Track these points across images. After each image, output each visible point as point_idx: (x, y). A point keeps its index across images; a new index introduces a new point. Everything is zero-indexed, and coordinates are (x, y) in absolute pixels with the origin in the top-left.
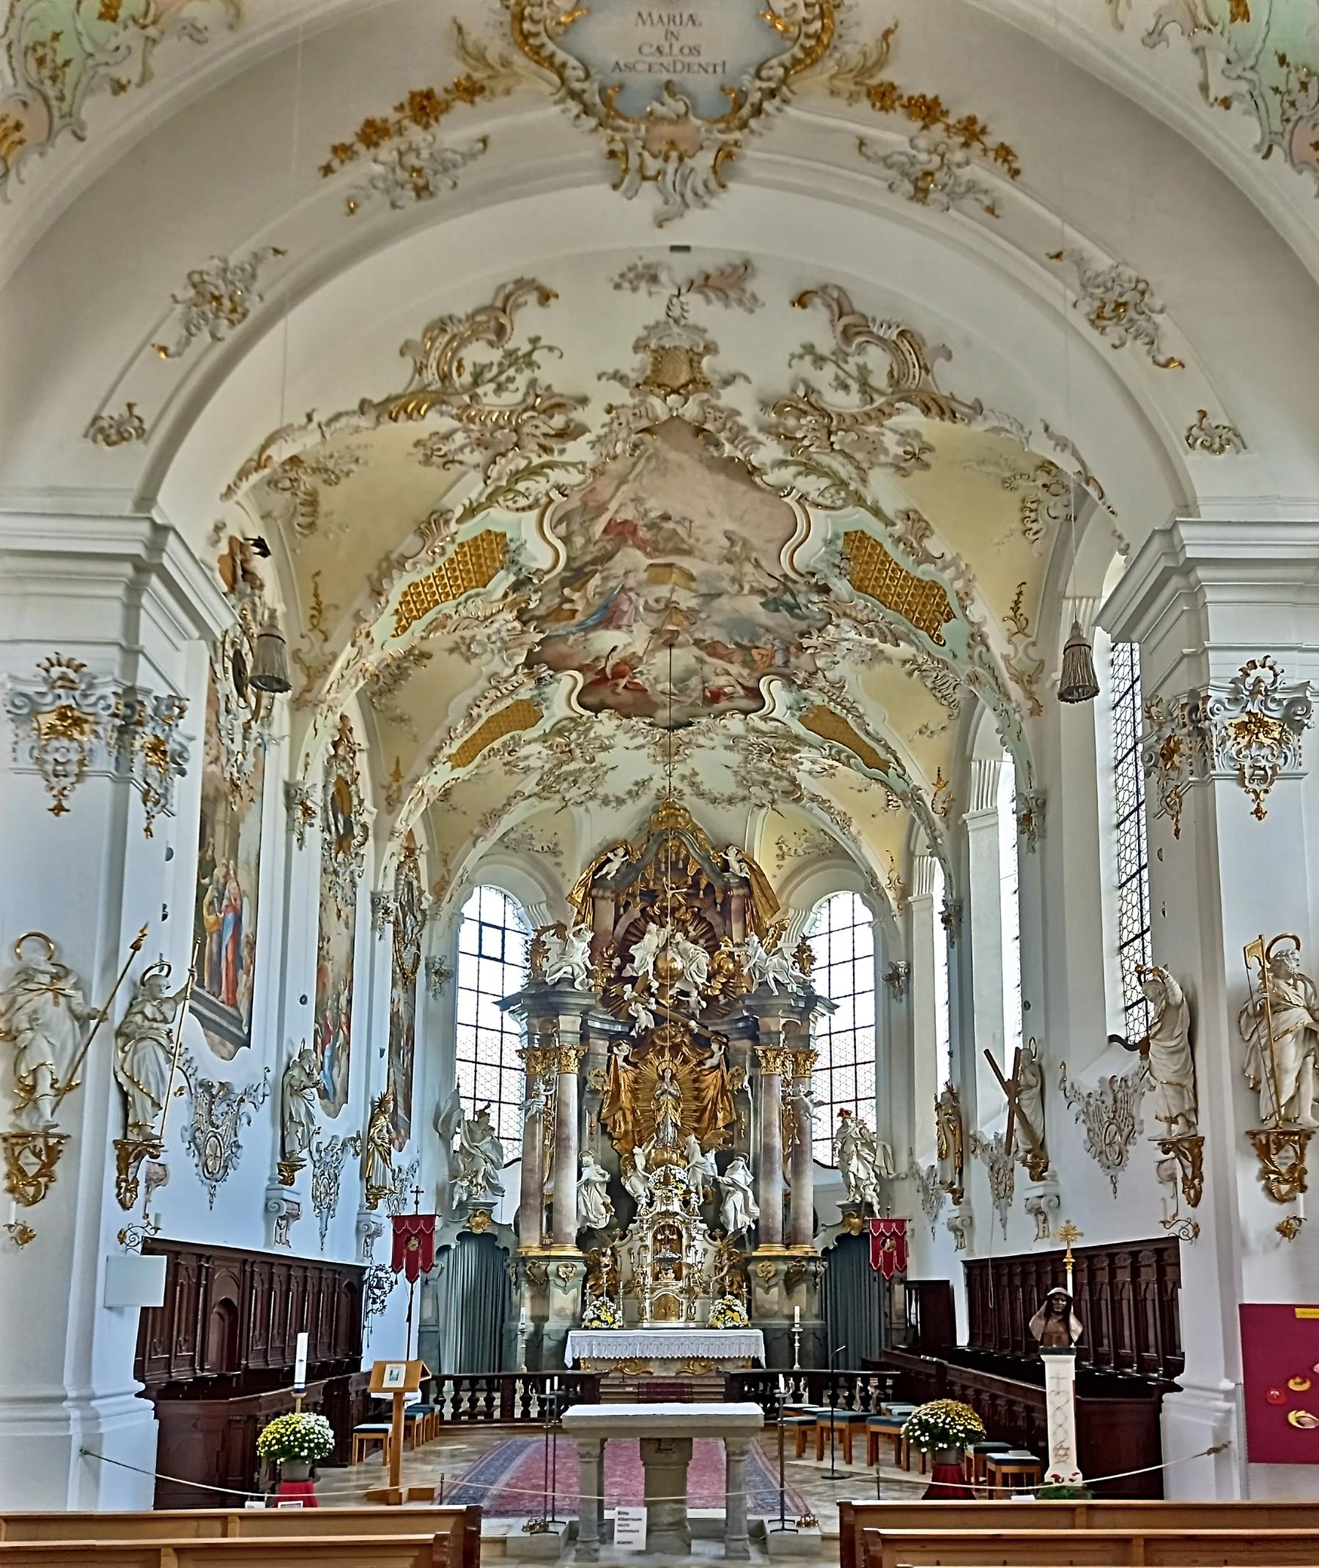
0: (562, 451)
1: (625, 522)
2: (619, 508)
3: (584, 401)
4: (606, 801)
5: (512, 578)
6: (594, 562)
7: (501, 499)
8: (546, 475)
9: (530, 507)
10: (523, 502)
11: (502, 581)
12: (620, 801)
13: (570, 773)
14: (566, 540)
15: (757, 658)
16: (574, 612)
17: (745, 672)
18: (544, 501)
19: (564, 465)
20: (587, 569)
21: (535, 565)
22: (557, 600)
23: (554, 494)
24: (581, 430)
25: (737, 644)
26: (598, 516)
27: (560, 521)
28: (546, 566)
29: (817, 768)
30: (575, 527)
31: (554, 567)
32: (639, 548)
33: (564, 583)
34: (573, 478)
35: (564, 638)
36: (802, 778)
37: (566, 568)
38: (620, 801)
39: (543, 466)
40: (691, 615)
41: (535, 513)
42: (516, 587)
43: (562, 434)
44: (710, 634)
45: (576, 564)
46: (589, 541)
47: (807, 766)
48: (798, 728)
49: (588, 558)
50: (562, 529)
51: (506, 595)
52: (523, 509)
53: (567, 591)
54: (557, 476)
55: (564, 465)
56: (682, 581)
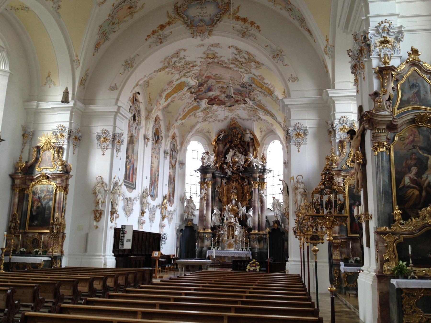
2: (207, 74)
3: (195, 62)
6: (204, 82)
11: (186, 89)
14: (198, 80)
16: (202, 90)
21: (192, 85)
24: (196, 66)
30: (199, 78)
33: (199, 86)
35: (202, 95)
37: (199, 84)
42: (189, 89)
43: (192, 66)
55: (194, 70)
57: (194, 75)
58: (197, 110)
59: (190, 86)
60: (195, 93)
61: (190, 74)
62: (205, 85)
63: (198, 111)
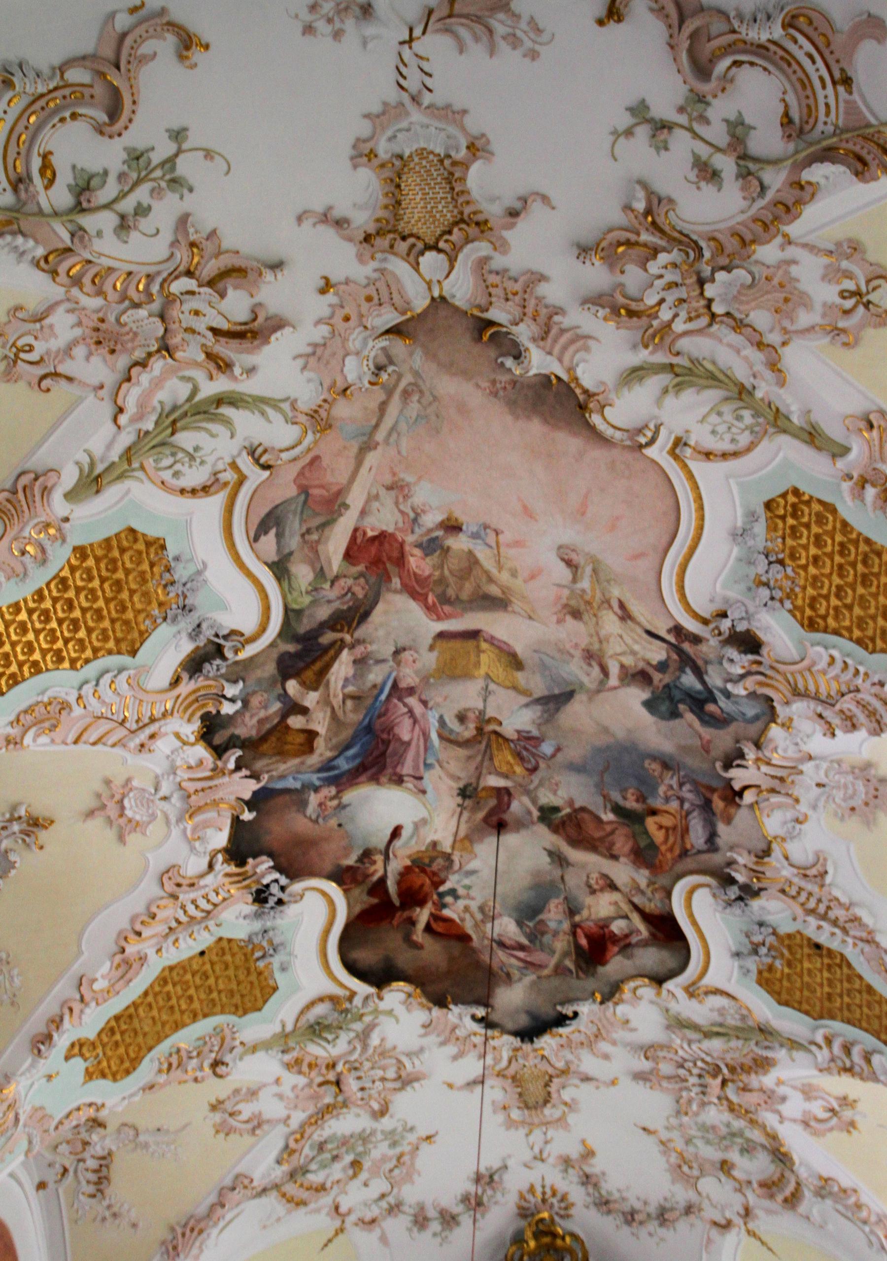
0: (250, 371)
1: (382, 537)
4: (420, 1221)
5: (187, 647)
7: (149, 463)
8: (227, 422)
9: (205, 490)
10: (195, 477)
12: (449, 1220)
13: (345, 1142)
14: (280, 569)
15: (658, 836)
17: (642, 877)
18: (229, 476)
19: (258, 404)
20: (328, 637)
22: (276, 706)
23: (246, 463)
25: (618, 810)
26: (328, 524)
27: (263, 528)
28: (248, 626)
29: (817, 1108)
31: (263, 628)
32: (414, 595)
33: (288, 667)
34: (278, 433)
36: (794, 1139)
38: (449, 1220)
39: (220, 401)
40: (525, 747)
41: (217, 501)
44: (568, 791)
45: (304, 626)
46: (321, 574)
47: (795, 1106)
48: (763, 1007)
49: (323, 613)
50: (269, 541)
51: (176, 682)
52: (194, 492)
53: (292, 686)
54: (248, 425)
55: (258, 404)
56: (499, 671)
57: (256, 476)
59: (208, 633)
60: (253, 749)
61: (215, 446)
62: (342, 668)
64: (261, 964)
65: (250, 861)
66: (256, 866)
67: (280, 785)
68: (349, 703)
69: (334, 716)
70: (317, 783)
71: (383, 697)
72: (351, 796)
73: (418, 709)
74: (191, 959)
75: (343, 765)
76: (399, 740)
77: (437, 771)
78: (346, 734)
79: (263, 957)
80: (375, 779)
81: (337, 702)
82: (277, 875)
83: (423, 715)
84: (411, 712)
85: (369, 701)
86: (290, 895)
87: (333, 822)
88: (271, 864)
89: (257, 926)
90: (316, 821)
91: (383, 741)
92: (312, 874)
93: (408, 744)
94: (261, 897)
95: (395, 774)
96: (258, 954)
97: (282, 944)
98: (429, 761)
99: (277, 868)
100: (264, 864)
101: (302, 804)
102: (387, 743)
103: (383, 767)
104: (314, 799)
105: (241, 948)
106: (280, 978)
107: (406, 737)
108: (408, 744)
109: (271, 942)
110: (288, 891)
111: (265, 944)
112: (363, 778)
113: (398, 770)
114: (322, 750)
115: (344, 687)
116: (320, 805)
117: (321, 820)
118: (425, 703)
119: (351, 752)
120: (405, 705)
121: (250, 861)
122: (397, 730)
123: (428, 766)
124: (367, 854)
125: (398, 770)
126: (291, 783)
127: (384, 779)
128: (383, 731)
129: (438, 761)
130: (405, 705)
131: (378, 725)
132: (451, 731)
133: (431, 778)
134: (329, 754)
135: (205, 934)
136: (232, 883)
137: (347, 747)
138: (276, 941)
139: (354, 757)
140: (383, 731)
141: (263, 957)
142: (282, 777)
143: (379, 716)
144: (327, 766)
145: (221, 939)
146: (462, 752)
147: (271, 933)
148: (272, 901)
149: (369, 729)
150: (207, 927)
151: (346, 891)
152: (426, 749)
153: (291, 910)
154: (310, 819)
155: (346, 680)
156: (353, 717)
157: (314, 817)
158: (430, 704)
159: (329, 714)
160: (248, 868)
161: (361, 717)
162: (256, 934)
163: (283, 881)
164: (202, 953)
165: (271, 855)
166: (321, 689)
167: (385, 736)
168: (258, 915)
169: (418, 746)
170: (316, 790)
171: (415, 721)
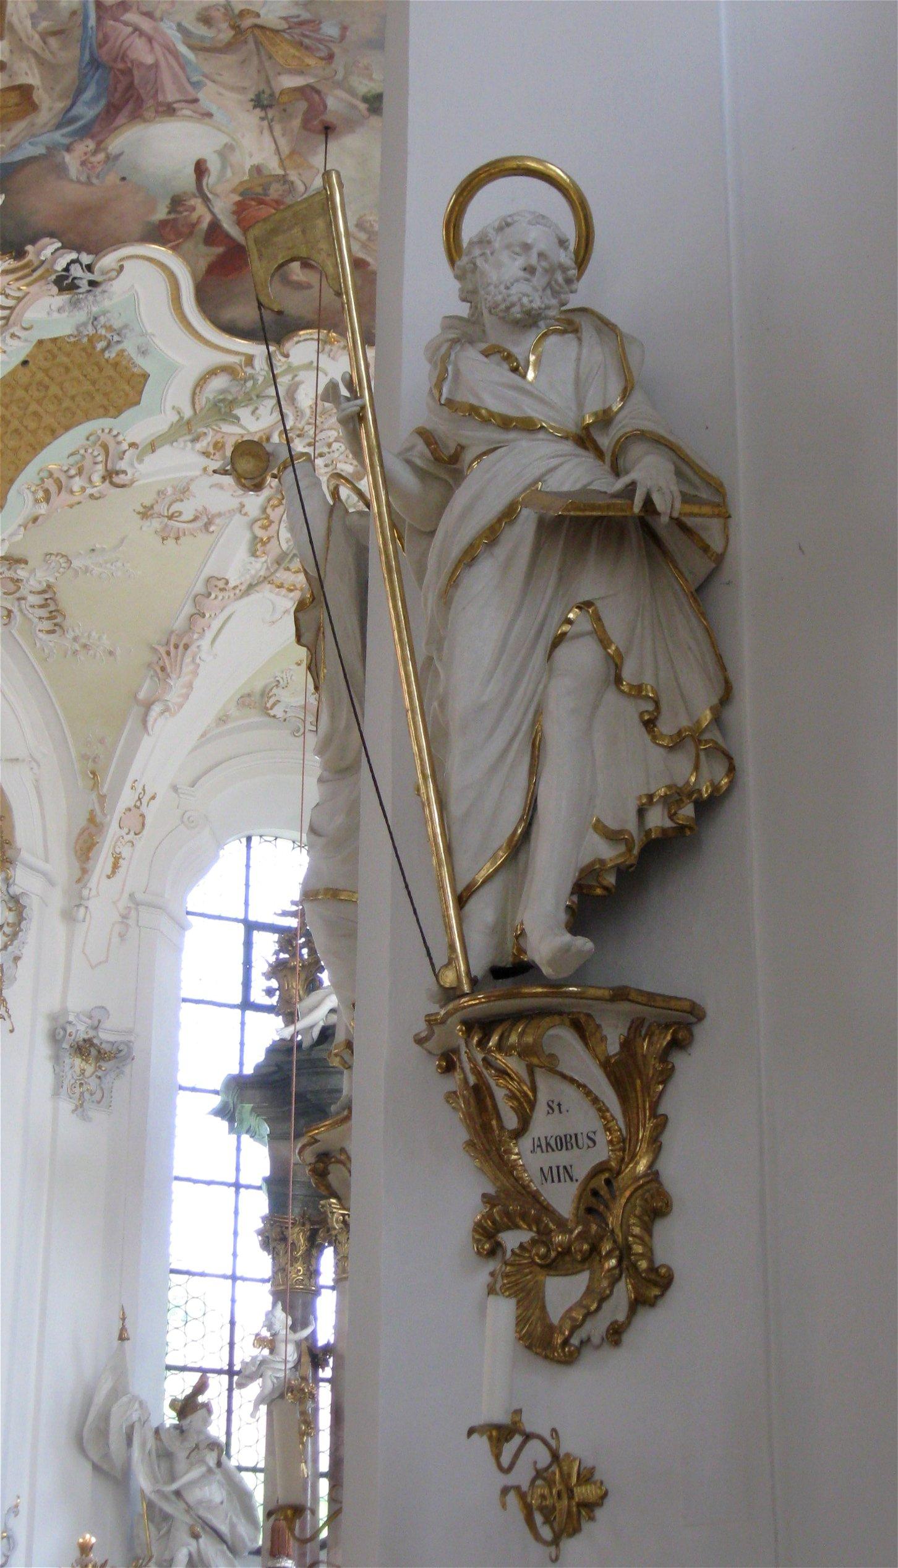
58: (114, 408)
63: (138, 425)
64: (111, 355)
65: (29, 248)
66: (38, 254)
67: (18, 156)
68: (53, 42)
69: (41, 62)
70: (66, 141)
71: (92, 22)
72: (117, 143)
73: (146, 24)
74: (13, 373)
75: (86, 111)
76: (141, 65)
77: (210, 87)
78: (69, 78)
79: (109, 346)
80: (137, 116)
81: (36, 43)
82: (74, 255)
83: (156, 29)
84: (136, 29)
85: (77, 33)
86: (103, 273)
87: (112, 178)
88: (60, 245)
89: (81, 316)
90: (89, 183)
91: (122, 72)
92: (119, 242)
93: (156, 66)
94: (65, 283)
95: (159, 104)
96: (100, 345)
97: (126, 326)
98: (195, 79)
99: (67, 246)
100: (48, 248)
101: (61, 170)
102: (128, 72)
103: (140, 102)
104: (72, 161)
105: (75, 344)
106: (144, 364)
107: (149, 60)
108: (156, 66)
109: (110, 329)
110: (96, 268)
111: (103, 332)
112: (121, 119)
113: (161, 98)
114: (49, 106)
115: (34, 25)
116: (83, 163)
117: (94, 181)
118: (149, 15)
119: (88, 95)
120: (126, 24)
121: (29, 248)
122: (133, 55)
123: (197, 85)
124: (177, 202)
125: (161, 98)
126: (29, 150)
127: (149, 114)
128: (115, 60)
129: (206, 76)
130: (126, 24)
131: (104, 55)
132: (203, 38)
133: (207, 97)
134: (60, 105)
135: (15, 343)
136: (17, 280)
137: (79, 92)
138: (117, 325)
139: (95, 100)
140: (115, 60)
141: (109, 346)
142: (15, 146)
143: (100, 46)
144: (65, 120)
145: (40, 342)
146: (229, 59)
147: (102, 320)
148: (84, 285)
149: (95, 63)
150: (13, 336)
151: (174, 248)
152: (183, 68)
153: (117, 287)
154: (79, 182)
155: (33, 16)
156: (69, 55)
157: (83, 178)
158: (158, 14)
159: (33, 60)
160: (30, 257)
161: (77, 52)
162: (84, 324)
163: (86, 259)
164: (25, 363)
165: (52, 235)
166: (6, 33)
167: (120, 66)
168: (75, 304)
169: (170, 67)
170: (68, 149)
171: (150, 40)
